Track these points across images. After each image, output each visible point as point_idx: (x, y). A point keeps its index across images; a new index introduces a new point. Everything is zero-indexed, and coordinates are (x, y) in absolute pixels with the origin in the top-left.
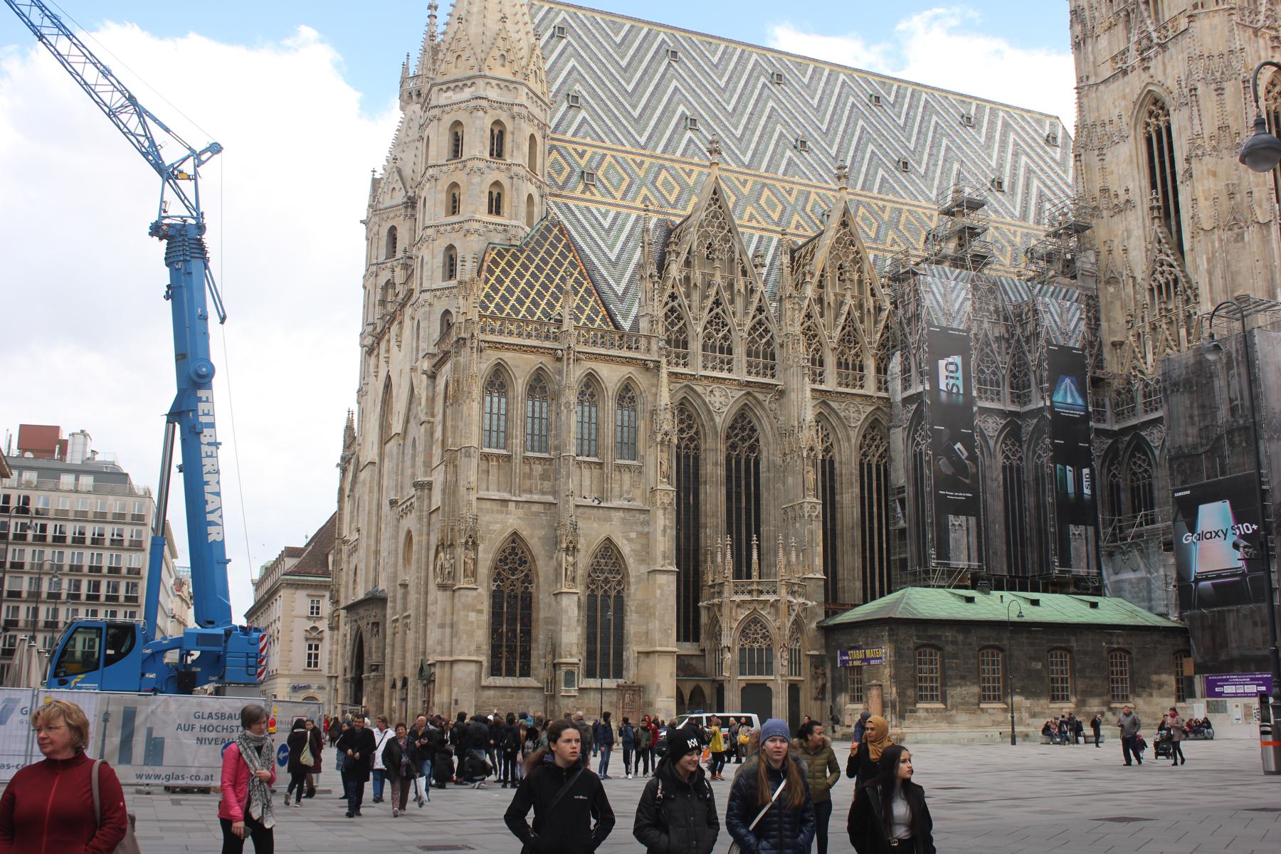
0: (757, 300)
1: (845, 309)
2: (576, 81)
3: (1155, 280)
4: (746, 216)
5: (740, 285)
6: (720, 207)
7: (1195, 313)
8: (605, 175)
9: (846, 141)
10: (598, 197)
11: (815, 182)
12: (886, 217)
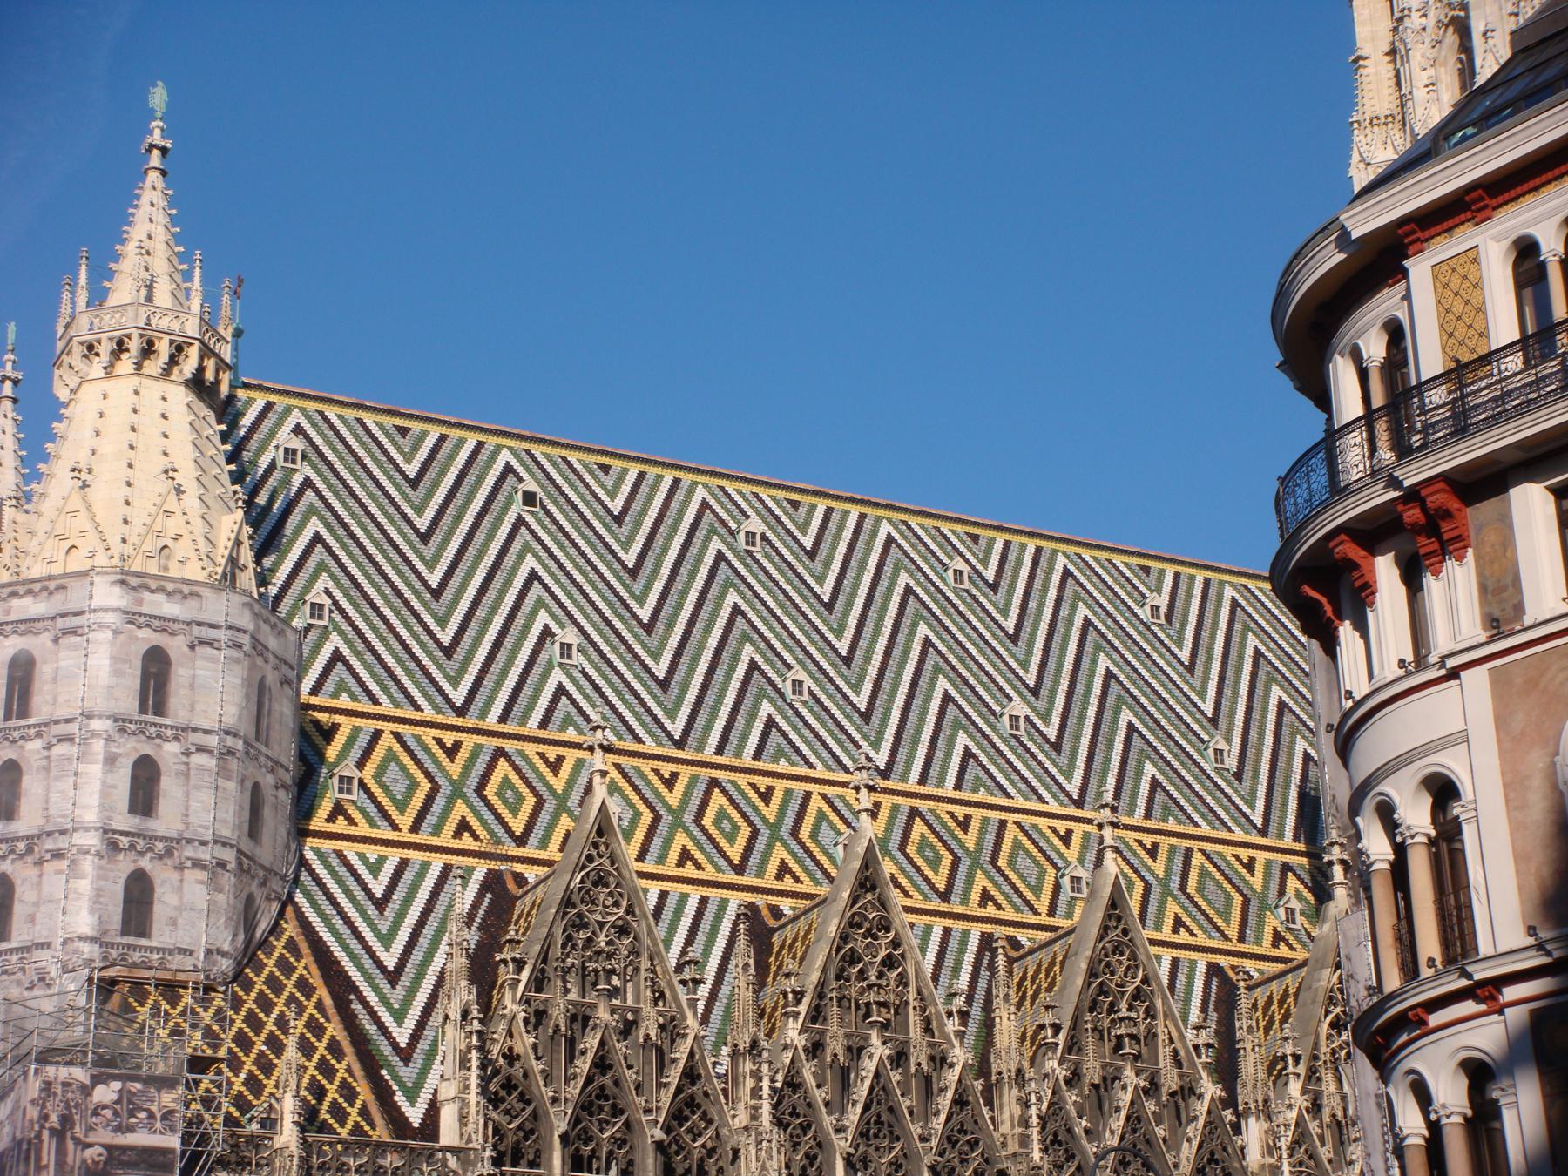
0: (685, 1056)
1: (870, 1066)
2: (321, 567)
4: (674, 855)
5: (650, 1027)
8: (378, 777)
9: (889, 674)
10: (363, 829)
11: (820, 772)
12: (970, 840)
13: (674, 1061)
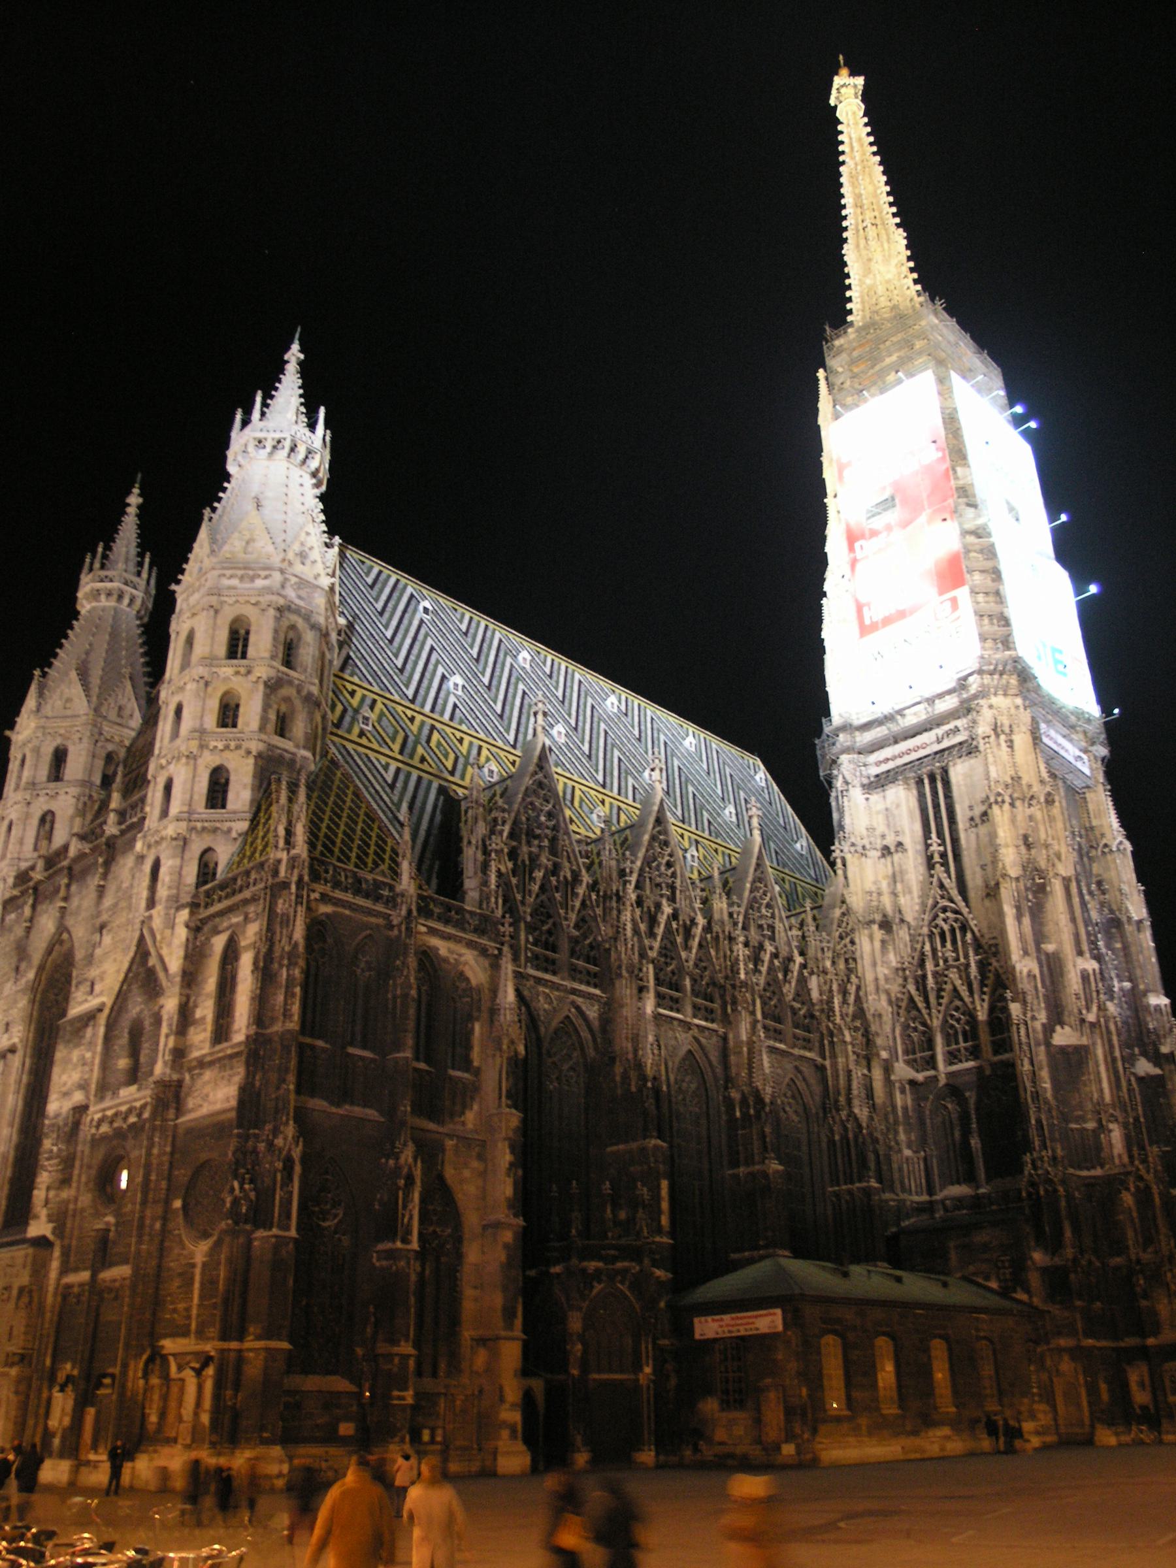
1: (665, 917)
3: (936, 926)
6: (545, 777)
7: (990, 964)
8: (379, 720)
9: (594, 741)
10: (375, 746)
11: (575, 777)
13: (577, 894)
